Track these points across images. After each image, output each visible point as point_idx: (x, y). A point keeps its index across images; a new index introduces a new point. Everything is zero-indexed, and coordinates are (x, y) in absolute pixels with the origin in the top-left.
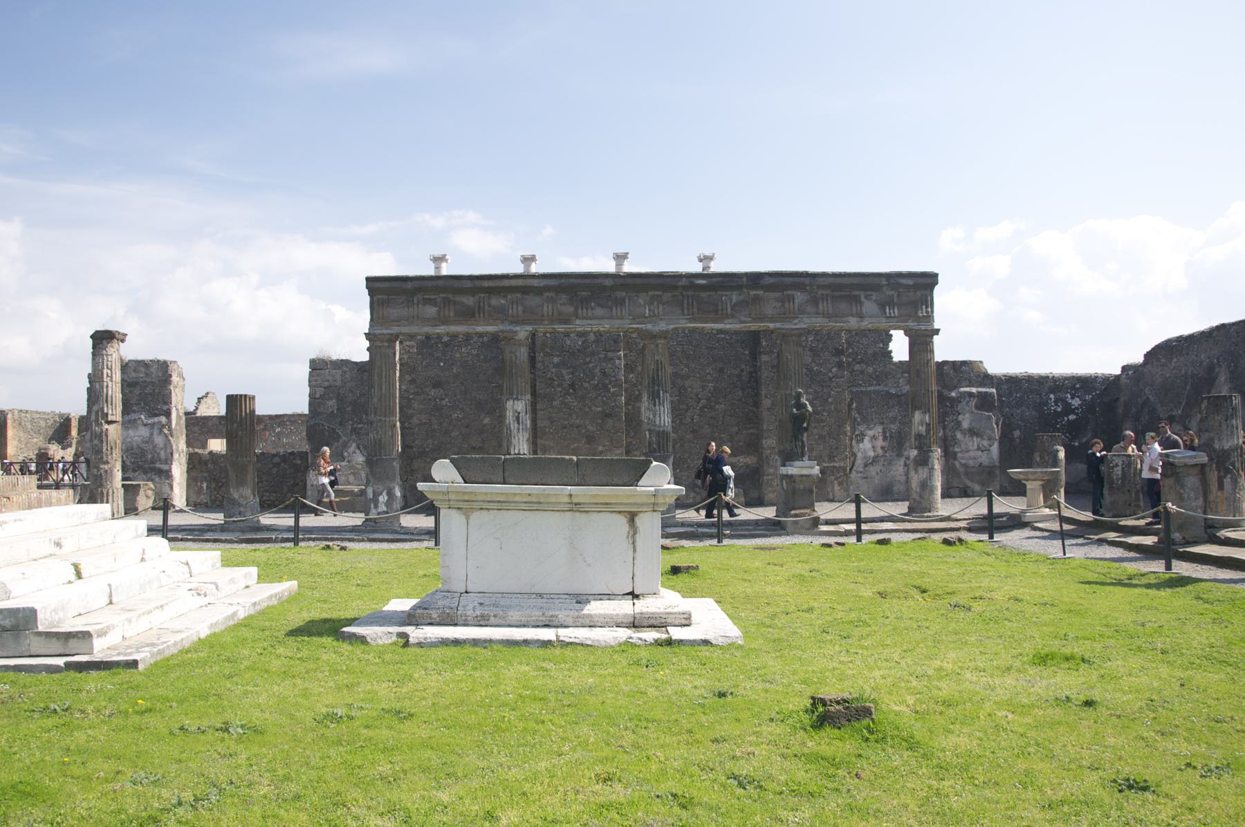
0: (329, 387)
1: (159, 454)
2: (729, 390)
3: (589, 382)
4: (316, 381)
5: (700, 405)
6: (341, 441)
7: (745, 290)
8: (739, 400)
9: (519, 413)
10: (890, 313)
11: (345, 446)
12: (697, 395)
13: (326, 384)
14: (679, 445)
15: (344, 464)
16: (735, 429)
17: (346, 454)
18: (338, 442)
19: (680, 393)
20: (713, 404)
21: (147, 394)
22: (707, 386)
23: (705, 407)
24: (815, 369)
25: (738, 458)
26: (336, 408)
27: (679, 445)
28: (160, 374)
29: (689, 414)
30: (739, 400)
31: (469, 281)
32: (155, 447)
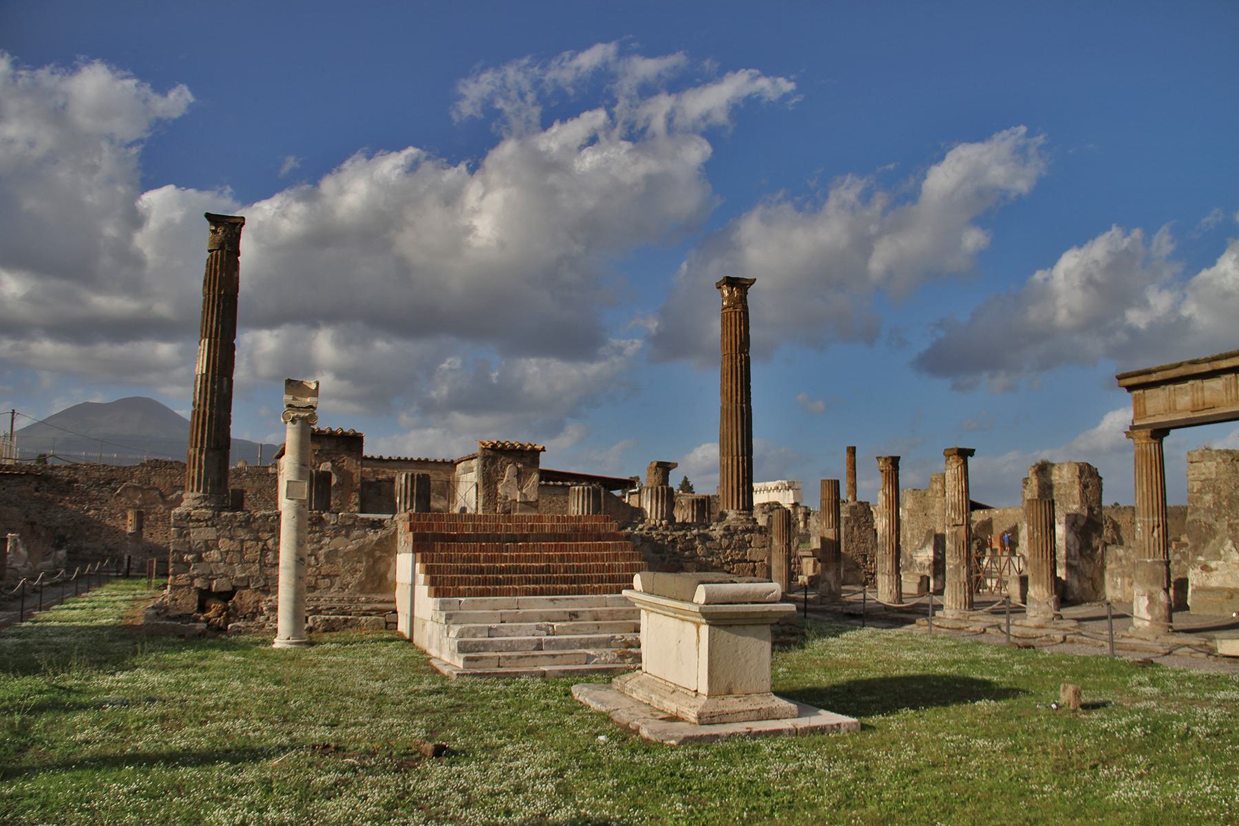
0: (1206, 479)
6: (1217, 538)
11: (1222, 544)
13: (1203, 477)
15: (1221, 562)
17: (1222, 552)
18: (1215, 538)
21: (1061, 495)
26: (1212, 502)
28: (1069, 476)
31: (1207, 364)
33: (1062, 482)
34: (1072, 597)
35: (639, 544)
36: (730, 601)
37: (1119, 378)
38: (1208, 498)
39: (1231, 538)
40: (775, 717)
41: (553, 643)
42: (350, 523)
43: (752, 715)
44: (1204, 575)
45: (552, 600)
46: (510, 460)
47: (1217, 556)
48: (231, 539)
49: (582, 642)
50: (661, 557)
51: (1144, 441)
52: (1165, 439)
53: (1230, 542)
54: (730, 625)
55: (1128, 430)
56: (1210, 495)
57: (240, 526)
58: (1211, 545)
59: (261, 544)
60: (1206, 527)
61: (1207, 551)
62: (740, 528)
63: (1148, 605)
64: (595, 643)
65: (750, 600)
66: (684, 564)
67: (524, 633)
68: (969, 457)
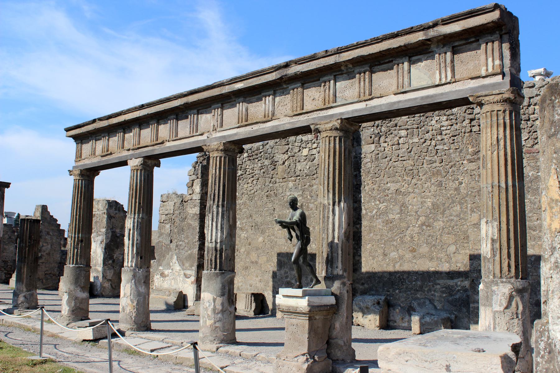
1: (98, 260)
2: (447, 205)
3: (313, 203)
4: (162, 210)
5: (419, 223)
6: (170, 253)
7: (285, 86)
8: (457, 216)
9: (130, 230)
10: (440, 80)
11: (172, 258)
12: (416, 212)
13: (166, 212)
14: (399, 264)
15: (170, 271)
16: (452, 248)
17: (171, 264)
19: (402, 210)
20: (431, 220)
22: (425, 202)
23: (423, 224)
24: (530, 174)
25: (456, 281)
27: (399, 264)
29: (408, 232)
30: (457, 216)
32: (97, 256)
33: (99, 213)
34: (96, 293)
37: (67, 130)
38: (168, 226)
39: (176, 254)
44: (161, 279)
47: (169, 266)
51: (78, 178)
52: (97, 179)
53: (176, 257)
55: (71, 169)
56: (169, 225)
58: (167, 258)
60: (164, 247)
61: (164, 263)
63: (67, 300)
68: (6, 189)
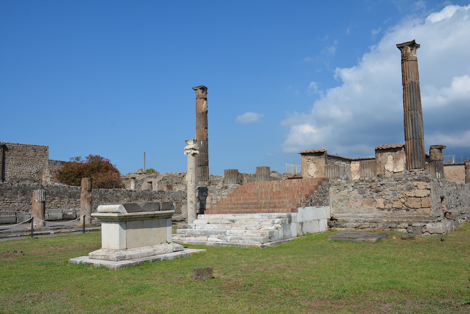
35: (352, 190)
36: (105, 211)
40: (109, 259)
41: (206, 232)
42: (236, 188)
43: (103, 257)
45: (234, 215)
46: (389, 153)
48: (203, 196)
49: (216, 232)
50: (363, 196)
54: (107, 221)
57: (205, 191)
59: (211, 197)
62: (409, 179)
64: (220, 233)
65: (110, 211)
66: (376, 199)
67: (206, 228)
